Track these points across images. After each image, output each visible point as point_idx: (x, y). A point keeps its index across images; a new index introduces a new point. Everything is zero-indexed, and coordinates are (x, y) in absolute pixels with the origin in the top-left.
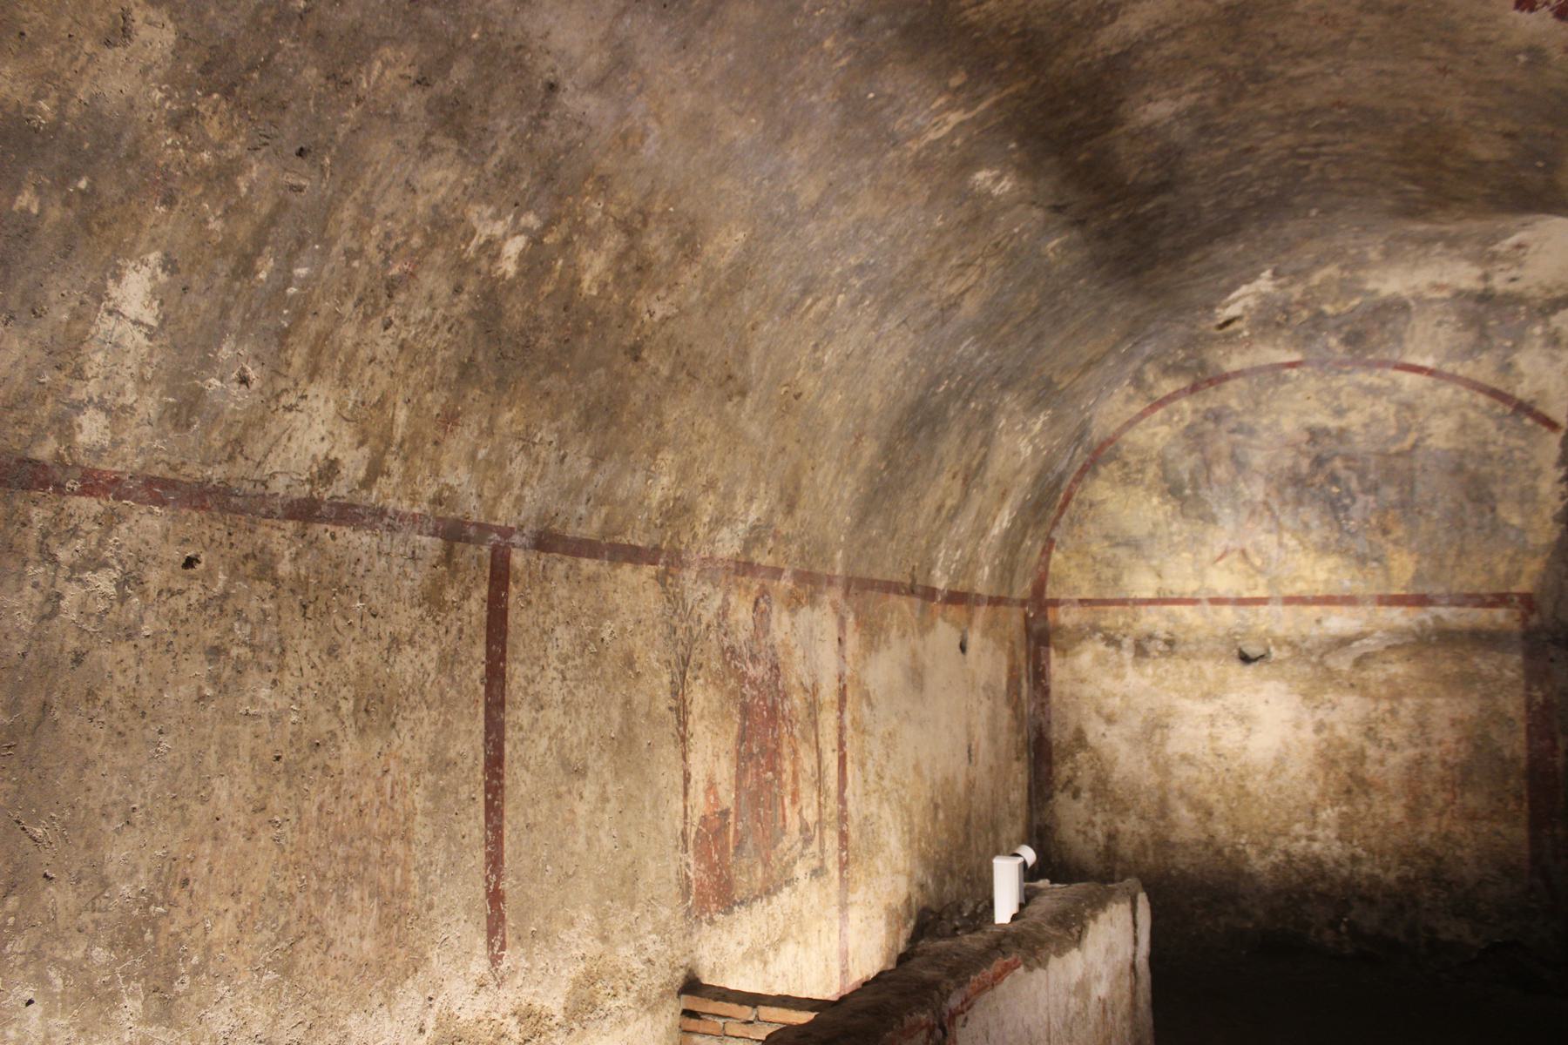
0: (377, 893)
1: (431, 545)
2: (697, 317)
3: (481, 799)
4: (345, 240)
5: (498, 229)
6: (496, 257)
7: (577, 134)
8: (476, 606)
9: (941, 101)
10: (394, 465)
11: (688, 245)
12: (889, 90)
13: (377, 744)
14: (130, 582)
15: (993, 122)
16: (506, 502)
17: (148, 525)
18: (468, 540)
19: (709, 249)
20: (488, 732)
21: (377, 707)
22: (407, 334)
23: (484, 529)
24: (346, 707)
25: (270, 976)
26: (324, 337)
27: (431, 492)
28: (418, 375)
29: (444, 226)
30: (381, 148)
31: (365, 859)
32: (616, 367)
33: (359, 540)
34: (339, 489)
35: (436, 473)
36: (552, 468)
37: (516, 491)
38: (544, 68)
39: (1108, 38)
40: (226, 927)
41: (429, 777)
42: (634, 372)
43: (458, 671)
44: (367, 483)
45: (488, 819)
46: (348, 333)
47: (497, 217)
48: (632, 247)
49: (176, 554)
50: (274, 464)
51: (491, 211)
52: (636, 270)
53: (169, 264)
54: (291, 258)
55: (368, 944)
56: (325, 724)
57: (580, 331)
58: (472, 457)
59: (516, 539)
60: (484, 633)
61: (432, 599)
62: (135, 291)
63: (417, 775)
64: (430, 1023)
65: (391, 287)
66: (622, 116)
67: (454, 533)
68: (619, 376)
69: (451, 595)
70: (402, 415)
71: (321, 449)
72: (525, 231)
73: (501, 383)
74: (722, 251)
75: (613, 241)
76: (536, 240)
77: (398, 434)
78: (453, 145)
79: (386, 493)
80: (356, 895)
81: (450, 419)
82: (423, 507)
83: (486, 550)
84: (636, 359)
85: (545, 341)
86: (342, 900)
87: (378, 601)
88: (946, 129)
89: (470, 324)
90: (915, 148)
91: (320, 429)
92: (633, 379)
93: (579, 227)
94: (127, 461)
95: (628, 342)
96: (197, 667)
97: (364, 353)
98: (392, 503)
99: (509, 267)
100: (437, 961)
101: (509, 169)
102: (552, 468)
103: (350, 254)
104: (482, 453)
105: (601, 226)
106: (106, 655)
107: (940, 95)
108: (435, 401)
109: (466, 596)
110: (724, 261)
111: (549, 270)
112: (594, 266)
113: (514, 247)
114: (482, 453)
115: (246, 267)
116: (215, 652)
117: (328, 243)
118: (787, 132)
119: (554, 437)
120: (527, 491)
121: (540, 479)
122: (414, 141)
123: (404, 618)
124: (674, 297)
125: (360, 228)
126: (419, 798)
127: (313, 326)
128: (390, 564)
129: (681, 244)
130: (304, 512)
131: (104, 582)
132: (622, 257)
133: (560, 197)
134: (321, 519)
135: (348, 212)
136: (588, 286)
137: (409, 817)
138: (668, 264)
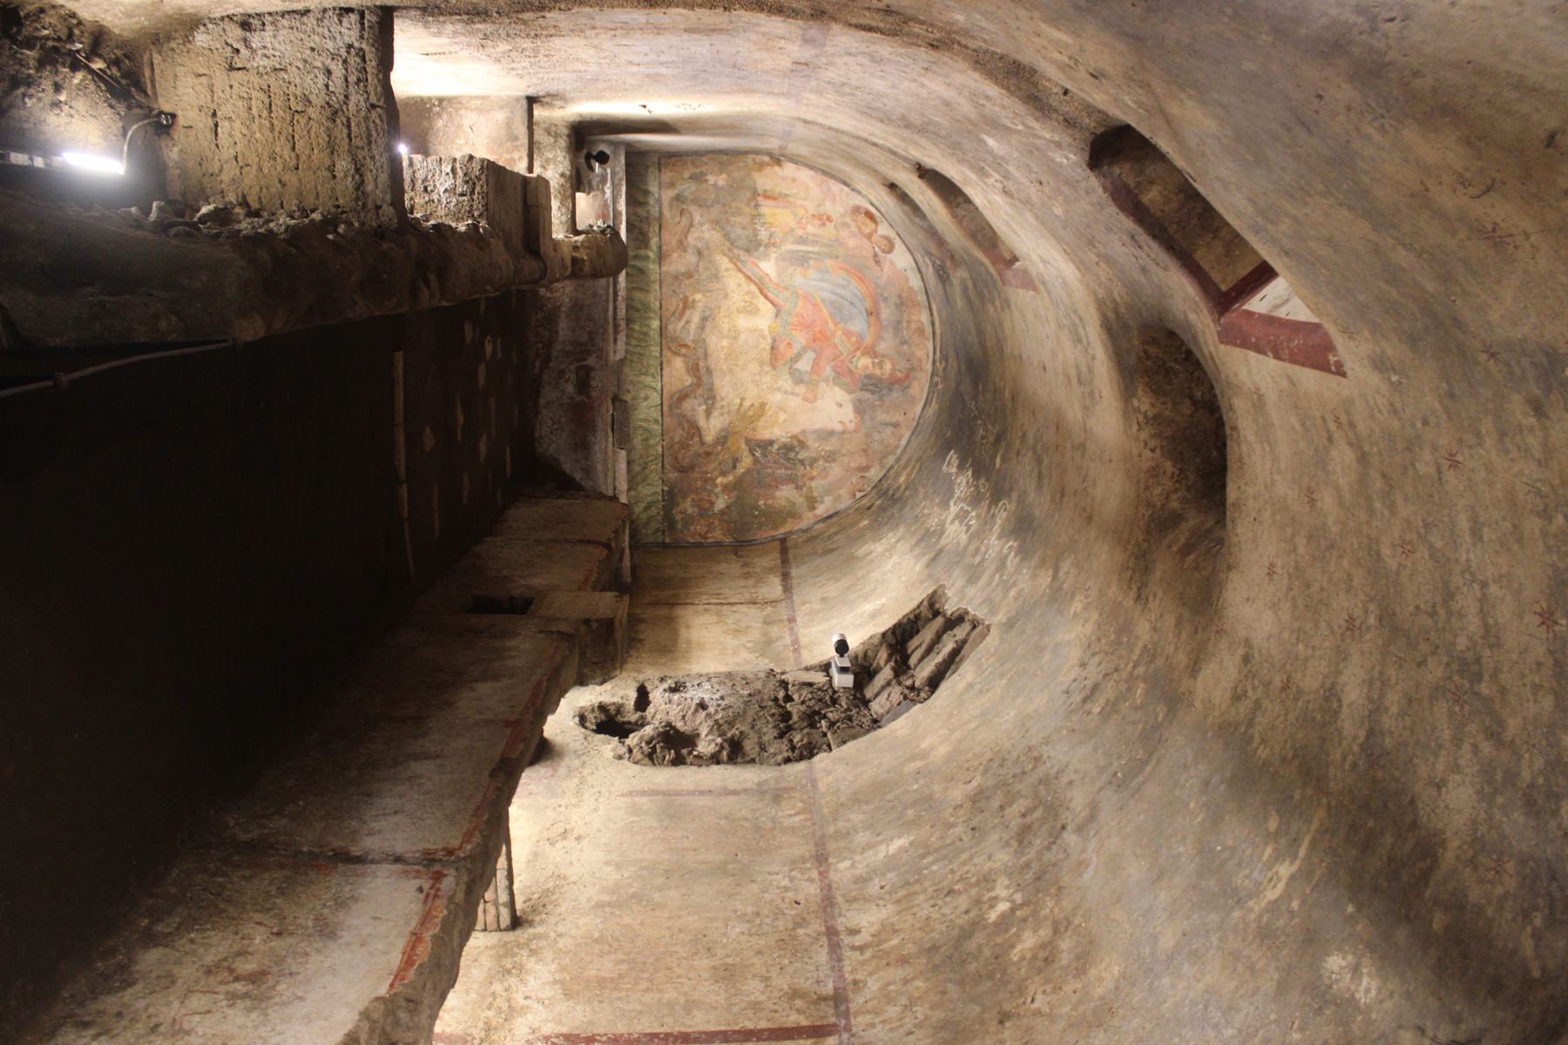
0: (621, 976)
1: (829, 988)
2: (1059, 1026)
3: (662, 1030)
4: (954, 866)
5: (1003, 893)
6: (992, 907)
7: (1061, 856)
8: (793, 1019)
9: (1269, 851)
10: (868, 954)
11: (1083, 962)
12: (1230, 843)
13: (705, 975)
14: (786, 889)
15: (1318, 873)
16: (868, 1019)
17: (812, 890)
18: (836, 1007)
19: (1093, 972)
20: (706, 1033)
21: (728, 974)
22: (935, 915)
23: (847, 1014)
24: (729, 961)
25: (596, 935)
26: (915, 893)
27: (859, 976)
28: (918, 934)
29: (987, 880)
30: (994, 837)
31: (642, 971)
32: (987, 1016)
33: (822, 956)
34: (847, 940)
35: (871, 974)
36: (902, 1031)
37: (877, 1020)
38: (1066, 817)
39: (1350, 726)
40: (627, 920)
41: (682, 1000)
42: (992, 1029)
43: (750, 1013)
44: (854, 948)
45: (646, 1035)
46: (921, 898)
47: (1007, 887)
48: (1051, 942)
49: (800, 898)
50: (849, 914)
51: (1007, 882)
52: (1045, 958)
53: (911, 843)
54: (935, 862)
55: (593, 972)
56: (720, 952)
57: (991, 976)
58: (888, 984)
59: (845, 1036)
60: (776, 1026)
61: (794, 994)
62: (898, 843)
63: (685, 994)
64: (528, 1002)
65: (950, 892)
66: (1084, 851)
67: (838, 998)
68: (982, 1022)
69: (799, 1003)
70: (895, 941)
71: (864, 923)
72: (1012, 901)
73: (936, 967)
74: (1100, 979)
75: (1045, 933)
76: (1013, 910)
77: (885, 946)
78: (1015, 844)
79: (850, 958)
80: (624, 967)
81: (904, 961)
82: (849, 977)
83: (833, 1020)
84: (1001, 1022)
85: (972, 967)
86: (623, 961)
87: (790, 970)
88: (1281, 886)
89: (956, 931)
90: (1256, 909)
91: (873, 919)
92: (987, 1032)
93: (1035, 914)
94: (833, 876)
95: (1007, 1007)
96: (749, 910)
97: (916, 909)
98: (846, 963)
99: (993, 916)
100: (563, 1007)
101: (1027, 866)
102: (902, 1031)
103: (952, 871)
104: (892, 988)
105: (1046, 918)
106: (755, 888)
107: (1266, 844)
108: (910, 948)
109: (799, 1012)
110: (1099, 991)
111: (1007, 931)
112: (1028, 942)
113: (1003, 907)
114: (892, 988)
115: (923, 856)
116: (758, 914)
117: (951, 862)
118: (1160, 877)
119: (921, 1017)
120: (879, 1027)
121: (892, 1030)
122: (1005, 837)
123: (781, 982)
124: (1052, 998)
125: (964, 863)
126: (670, 995)
127: (917, 888)
128: (815, 972)
129: (1078, 957)
130: (831, 932)
131: (786, 882)
132: (1043, 946)
133: (1038, 891)
134: (830, 940)
135: (964, 856)
136: (1015, 955)
137: (660, 991)
138: (1063, 968)
